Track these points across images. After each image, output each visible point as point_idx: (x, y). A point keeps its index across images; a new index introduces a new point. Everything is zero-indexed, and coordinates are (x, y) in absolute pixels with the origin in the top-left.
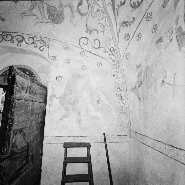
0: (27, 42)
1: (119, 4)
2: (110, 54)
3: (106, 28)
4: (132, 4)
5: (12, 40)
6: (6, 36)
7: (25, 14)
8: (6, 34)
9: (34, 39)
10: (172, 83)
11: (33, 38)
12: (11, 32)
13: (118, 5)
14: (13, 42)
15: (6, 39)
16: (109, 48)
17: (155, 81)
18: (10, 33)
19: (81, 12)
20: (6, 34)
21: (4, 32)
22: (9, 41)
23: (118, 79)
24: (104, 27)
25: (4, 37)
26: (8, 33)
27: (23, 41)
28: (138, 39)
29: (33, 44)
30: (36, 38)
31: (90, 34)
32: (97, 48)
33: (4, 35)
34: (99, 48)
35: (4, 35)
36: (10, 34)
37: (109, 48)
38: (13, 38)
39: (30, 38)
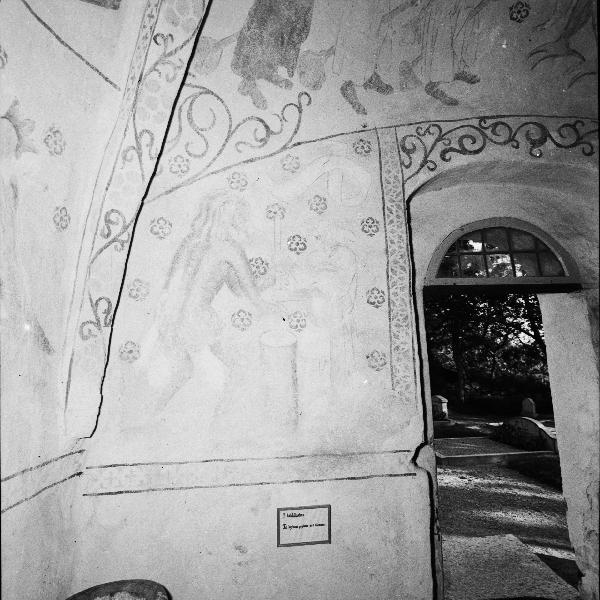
0: (559, 140)
5: (511, 139)
6: (491, 129)
7: (543, 54)
8: (490, 122)
9: (576, 131)
11: (573, 126)
12: (504, 116)
14: (517, 147)
15: (494, 137)
18: (503, 120)
20: (490, 122)
21: (483, 119)
22: (505, 143)
25: (488, 132)
26: (494, 121)
27: (545, 140)
29: (578, 149)
30: (583, 125)
33: (486, 128)
35: (486, 128)
36: (503, 123)
38: (515, 134)
39: (563, 126)
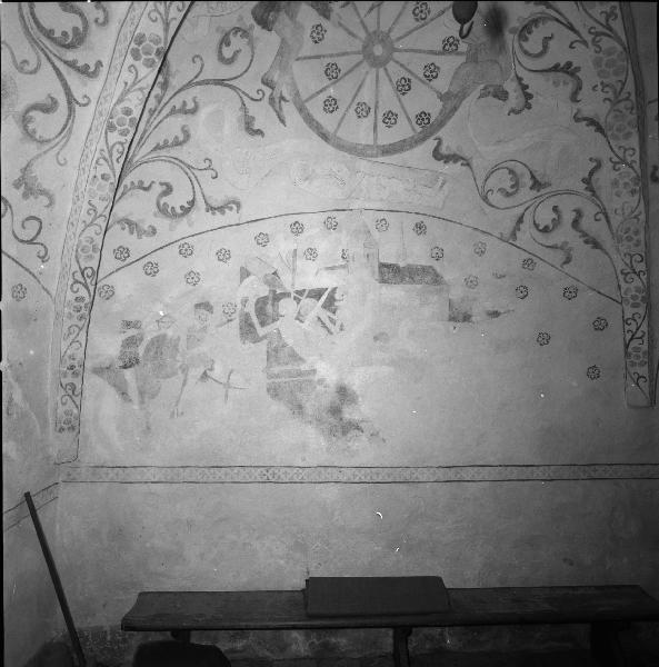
1: (136, 184)
2: (76, 282)
3: (98, 221)
4: (162, 203)
10: (224, 380)
13: (132, 183)
16: (83, 267)
17: (185, 370)
19: (31, 126)
23: (75, 345)
24: (95, 218)
28: (149, 271)
31: (25, 196)
32: (22, 241)
34: (31, 242)
37: (83, 267)
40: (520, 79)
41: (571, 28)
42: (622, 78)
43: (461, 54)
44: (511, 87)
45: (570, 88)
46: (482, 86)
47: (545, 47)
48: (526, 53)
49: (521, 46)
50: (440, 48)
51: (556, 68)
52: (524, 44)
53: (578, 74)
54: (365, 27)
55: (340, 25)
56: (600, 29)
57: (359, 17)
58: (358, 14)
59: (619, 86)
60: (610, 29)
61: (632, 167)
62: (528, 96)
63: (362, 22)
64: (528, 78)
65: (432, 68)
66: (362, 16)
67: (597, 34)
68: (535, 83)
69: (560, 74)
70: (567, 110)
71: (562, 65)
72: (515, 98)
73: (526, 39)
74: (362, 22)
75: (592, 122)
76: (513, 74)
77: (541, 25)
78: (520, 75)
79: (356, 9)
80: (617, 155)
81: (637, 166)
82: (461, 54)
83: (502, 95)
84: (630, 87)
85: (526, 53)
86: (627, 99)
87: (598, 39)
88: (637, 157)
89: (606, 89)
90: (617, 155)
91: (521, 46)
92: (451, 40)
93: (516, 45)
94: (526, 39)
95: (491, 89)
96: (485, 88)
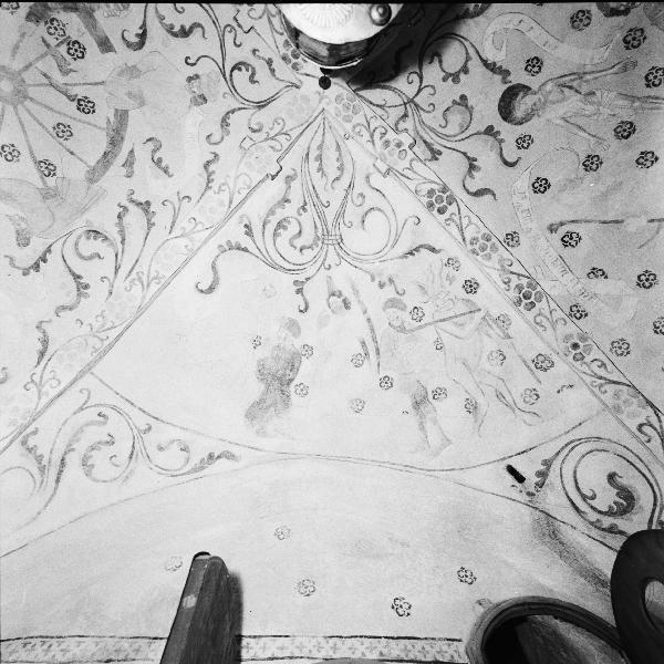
40: (49, 250)
41: (117, 270)
42: (117, 322)
43: (45, 183)
44: (37, 246)
45: (67, 301)
46: (22, 215)
47: (91, 258)
48: (76, 244)
49: (80, 237)
50: (38, 159)
51: (77, 277)
52: (83, 238)
53: (82, 299)
54: (27, 67)
55: (23, 35)
56: (144, 279)
57: (37, 59)
58: (37, 59)
59: (109, 325)
60: (148, 285)
61: (40, 398)
62: (36, 267)
63: (30, 65)
64: (53, 258)
65: (16, 153)
66: (39, 65)
67: (140, 278)
68: (54, 264)
69: (74, 285)
70: (46, 311)
71: (82, 281)
72: (28, 256)
73: (88, 238)
74: (30, 65)
75: (45, 342)
76: (50, 241)
77: (106, 243)
78: (52, 248)
79: (42, 56)
80: (41, 377)
81: (44, 400)
82: (45, 183)
83: (23, 240)
84: (113, 334)
85: (76, 244)
86: (102, 340)
87: (137, 282)
88: (53, 393)
89: (100, 319)
90: (41, 377)
91: (80, 237)
92: (51, 167)
93: (79, 232)
94: (88, 238)
95: (23, 226)
96: (22, 219)
